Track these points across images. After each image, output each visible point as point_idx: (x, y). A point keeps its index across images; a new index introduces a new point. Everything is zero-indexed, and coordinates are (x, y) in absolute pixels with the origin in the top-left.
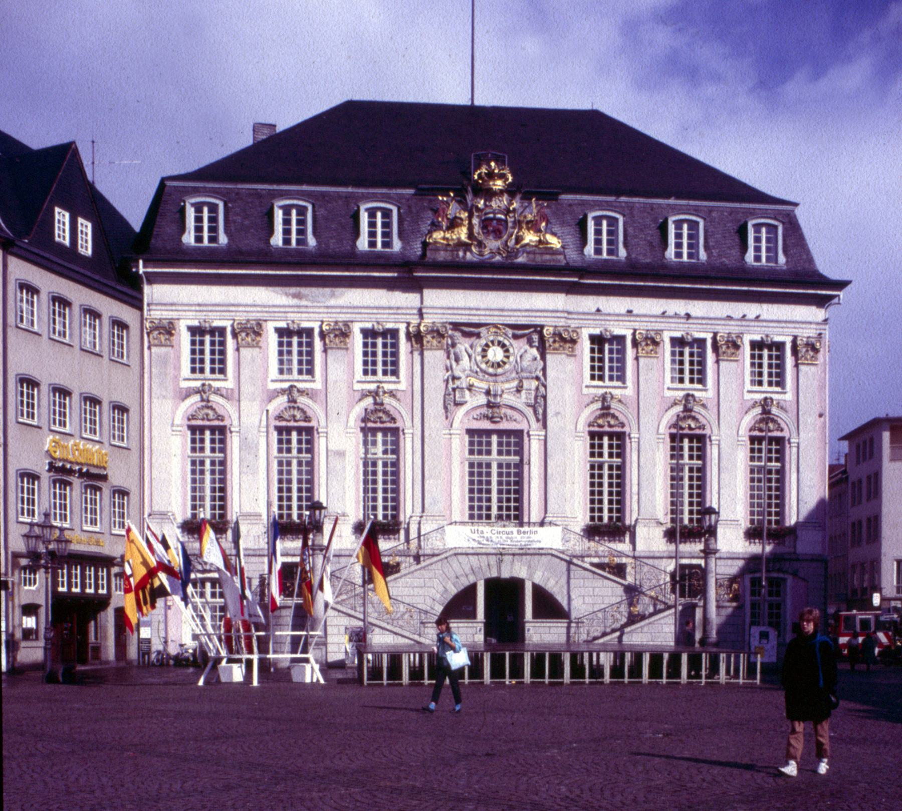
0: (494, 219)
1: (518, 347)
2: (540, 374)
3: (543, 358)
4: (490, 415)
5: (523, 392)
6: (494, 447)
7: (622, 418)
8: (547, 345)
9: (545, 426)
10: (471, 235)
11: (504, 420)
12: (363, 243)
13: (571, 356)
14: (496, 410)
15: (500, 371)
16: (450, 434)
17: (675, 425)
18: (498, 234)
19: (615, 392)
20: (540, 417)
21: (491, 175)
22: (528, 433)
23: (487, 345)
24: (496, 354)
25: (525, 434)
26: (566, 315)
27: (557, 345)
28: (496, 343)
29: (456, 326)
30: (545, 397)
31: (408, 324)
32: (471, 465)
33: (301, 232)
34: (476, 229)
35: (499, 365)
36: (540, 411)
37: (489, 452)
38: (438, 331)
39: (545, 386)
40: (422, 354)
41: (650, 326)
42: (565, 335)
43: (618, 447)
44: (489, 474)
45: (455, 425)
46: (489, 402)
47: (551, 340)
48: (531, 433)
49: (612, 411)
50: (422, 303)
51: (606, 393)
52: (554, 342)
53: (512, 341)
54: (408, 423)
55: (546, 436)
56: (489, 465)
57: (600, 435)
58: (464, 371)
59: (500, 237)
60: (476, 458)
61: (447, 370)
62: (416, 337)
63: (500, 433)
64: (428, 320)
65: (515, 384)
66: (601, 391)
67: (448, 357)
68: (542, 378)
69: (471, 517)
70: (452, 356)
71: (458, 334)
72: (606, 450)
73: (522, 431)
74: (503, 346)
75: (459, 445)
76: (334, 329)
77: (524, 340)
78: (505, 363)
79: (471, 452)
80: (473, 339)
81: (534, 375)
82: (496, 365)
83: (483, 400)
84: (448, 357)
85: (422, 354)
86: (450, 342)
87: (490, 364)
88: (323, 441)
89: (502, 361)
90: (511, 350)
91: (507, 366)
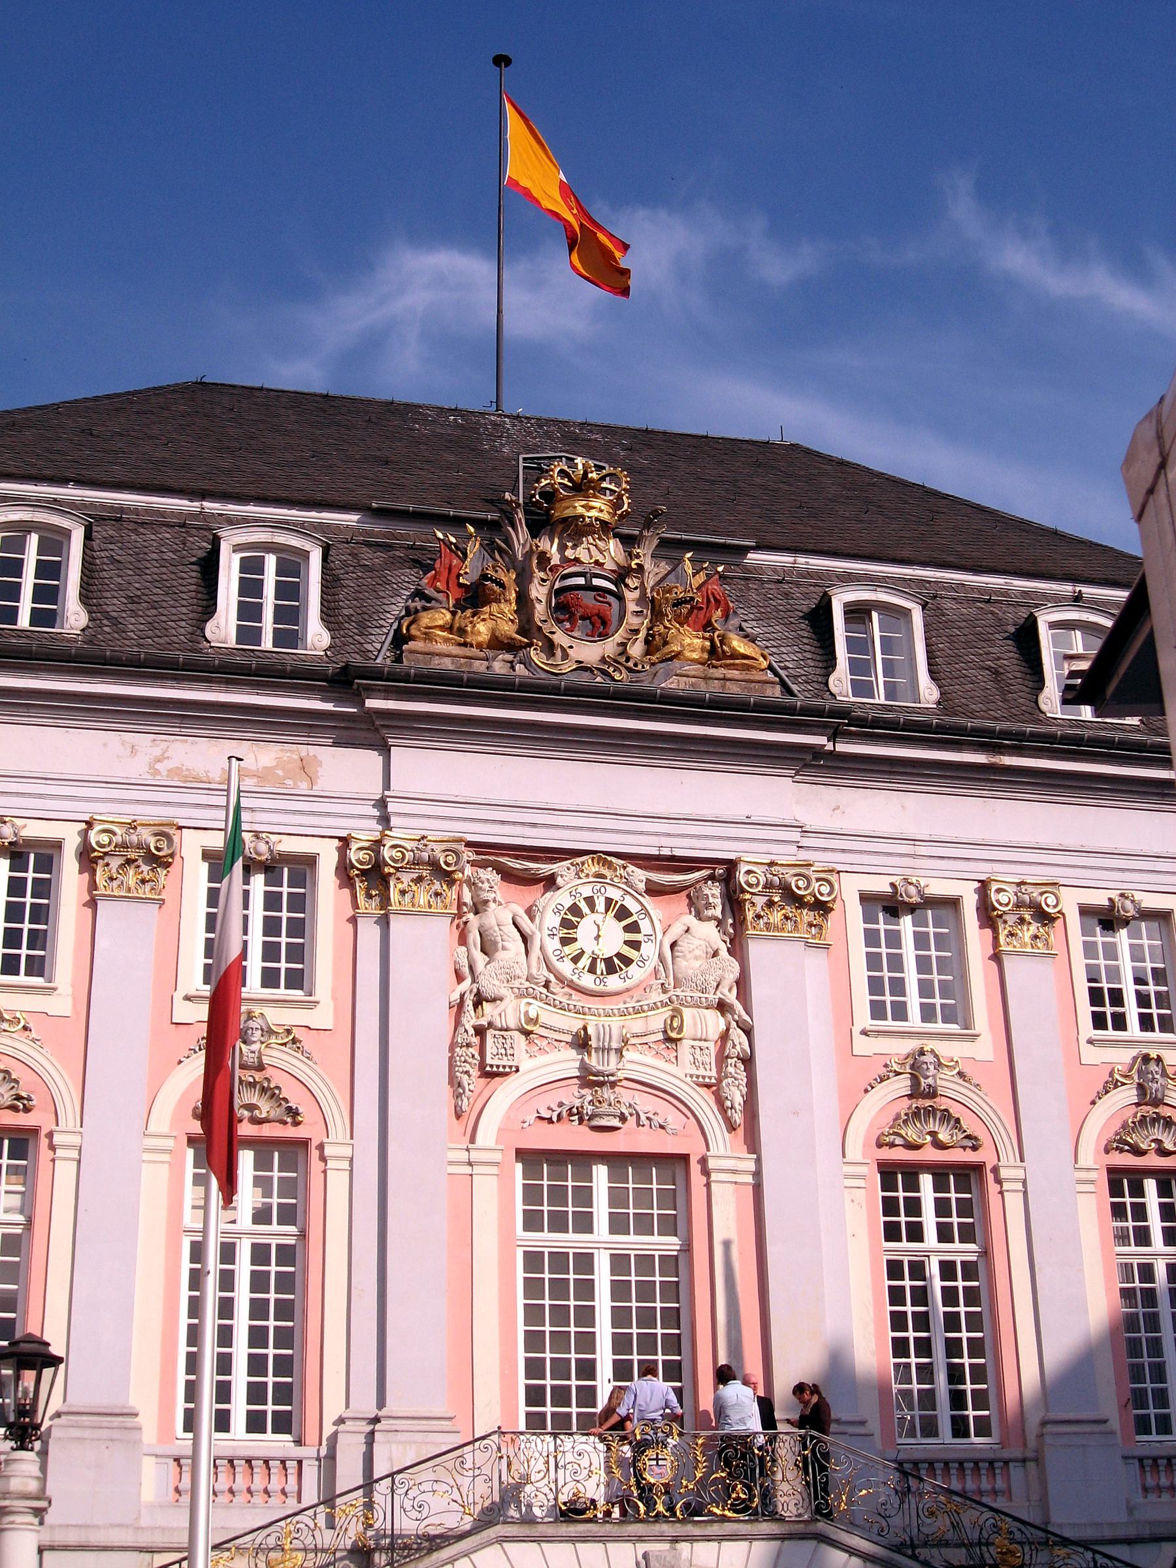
1: (661, 919)
2: (731, 997)
3: (737, 947)
4: (589, 1109)
5: (685, 1046)
6: (601, 1209)
7: (970, 1124)
8: (750, 915)
9: (753, 1143)
10: (527, 627)
11: (632, 1121)
12: (224, 627)
13: (817, 946)
14: (606, 1093)
15: (614, 982)
16: (470, 1164)
17: (1118, 1144)
18: (600, 627)
19: (946, 1049)
20: (738, 1118)
21: (582, 487)
22: (703, 1161)
23: (575, 910)
24: (602, 935)
25: (695, 1168)
26: (795, 835)
27: (776, 917)
28: (600, 905)
29: (487, 852)
30: (748, 1062)
31: (345, 842)
32: (533, 1260)
33: (47, 594)
34: (540, 610)
35: (611, 969)
36: (736, 1096)
37: (585, 1224)
38: (434, 864)
39: (748, 1032)
40: (384, 922)
41: (1033, 874)
42: (798, 886)
43: (965, 1208)
44: (586, 1289)
45: (487, 1134)
46: (584, 1068)
47: (760, 901)
48: (712, 1164)
49: (943, 1103)
50: (387, 785)
51: (922, 1053)
52: (770, 904)
53: (647, 901)
54: (339, 1130)
55: (758, 1174)
56: (585, 1262)
57: (911, 1173)
58: (512, 978)
59: (604, 636)
60: (547, 1240)
61: (460, 978)
62: (370, 876)
63: (616, 1160)
64: (403, 831)
65: (657, 1021)
66: (908, 1046)
67: (463, 940)
68: (738, 1007)
69: (535, 1423)
70: (474, 937)
71: (489, 876)
72: (929, 1220)
73: (685, 1158)
74: (623, 913)
75: (498, 1195)
76: (124, 845)
77: (681, 900)
78: (627, 961)
79: (532, 1222)
80: (532, 894)
81: (713, 998)
82: (601, 966)
83: (567, 1062)
84: (463, 940)
85: (384, 922)
86: (467, 897)
87: (585, 962)
88: (65, 1172)
89: (618, 955)
90: (645, 926)
91: (636, 973)
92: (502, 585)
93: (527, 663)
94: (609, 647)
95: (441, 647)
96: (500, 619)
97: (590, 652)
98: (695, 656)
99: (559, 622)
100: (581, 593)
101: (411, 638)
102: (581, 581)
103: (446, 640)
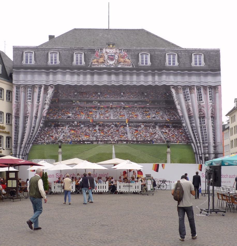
0: (111, 55)
18: (112, 59)
59: (113, 60)
92: (102, 55)
93: (104, 64)
94: (114, 62)
95: (96, 63)
96: (101, 60)
97: (111, 63)
98: (123, 62)
99: (108, 59)
100: (110, 56)
101: (93, 63)
102: (110, 54)
103: (96, 63)
